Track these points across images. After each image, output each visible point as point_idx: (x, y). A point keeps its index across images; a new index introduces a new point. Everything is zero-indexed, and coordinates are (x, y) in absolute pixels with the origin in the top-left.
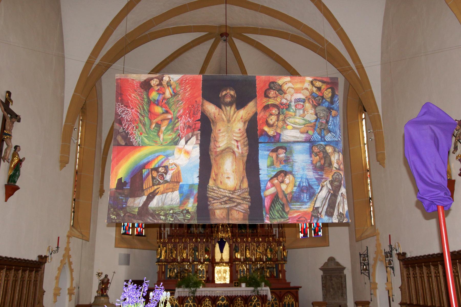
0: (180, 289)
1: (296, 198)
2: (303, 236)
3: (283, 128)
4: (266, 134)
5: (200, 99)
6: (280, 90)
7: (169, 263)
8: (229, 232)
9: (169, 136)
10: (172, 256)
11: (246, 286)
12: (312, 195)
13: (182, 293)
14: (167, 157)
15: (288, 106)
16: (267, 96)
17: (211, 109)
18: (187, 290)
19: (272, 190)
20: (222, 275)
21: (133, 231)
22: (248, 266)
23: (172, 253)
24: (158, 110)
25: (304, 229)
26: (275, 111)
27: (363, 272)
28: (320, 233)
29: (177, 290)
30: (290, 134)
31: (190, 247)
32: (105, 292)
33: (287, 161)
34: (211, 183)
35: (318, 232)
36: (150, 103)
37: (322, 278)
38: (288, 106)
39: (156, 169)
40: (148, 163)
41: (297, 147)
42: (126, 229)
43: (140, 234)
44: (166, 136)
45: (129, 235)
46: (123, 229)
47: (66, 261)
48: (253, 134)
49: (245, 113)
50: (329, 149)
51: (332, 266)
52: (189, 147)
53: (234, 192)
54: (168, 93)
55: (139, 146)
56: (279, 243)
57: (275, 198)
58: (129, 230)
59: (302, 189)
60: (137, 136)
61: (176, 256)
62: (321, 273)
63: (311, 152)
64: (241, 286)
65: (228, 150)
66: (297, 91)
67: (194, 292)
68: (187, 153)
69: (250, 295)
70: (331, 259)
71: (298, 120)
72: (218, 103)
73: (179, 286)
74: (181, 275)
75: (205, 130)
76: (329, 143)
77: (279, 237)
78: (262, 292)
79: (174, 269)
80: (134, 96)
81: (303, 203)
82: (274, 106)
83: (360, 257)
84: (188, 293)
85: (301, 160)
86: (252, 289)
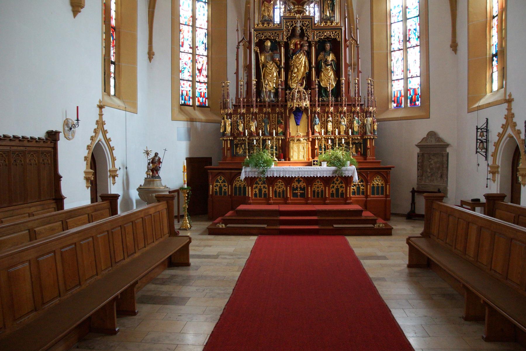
0: (248, 169)
2: (397, 106)
8: (307, 99)
10: (238, 129)
11: (327, 166)
13: (250, 173)
18: (255, 170)
20: (299, 152)
21: (194, 102)
22: (330, 141)
23: (238, 125)
25: (397, 97)
27: (479, 150)
31: (259, 118)
32: (157, 173)
35: (415, 101)
37: (418, 156)
42: (185, 100)
43: (202, 106)
45: (189, 106)
46: (182, 100)
47: (100, 136)
51: (434, 143)
56: (367, 114)
58: (189, 100)
61: (244, 129)
62: (418, 150)
64: (321, 165)
67: (263, 172)
69: (333, 176)
73: (247, 165)
74: (249, 152)
77: (368, 106)
78: (346, 172)
79: (241, 144)
83: (477, 132)
84: (256, 173)
86: (334, 168)
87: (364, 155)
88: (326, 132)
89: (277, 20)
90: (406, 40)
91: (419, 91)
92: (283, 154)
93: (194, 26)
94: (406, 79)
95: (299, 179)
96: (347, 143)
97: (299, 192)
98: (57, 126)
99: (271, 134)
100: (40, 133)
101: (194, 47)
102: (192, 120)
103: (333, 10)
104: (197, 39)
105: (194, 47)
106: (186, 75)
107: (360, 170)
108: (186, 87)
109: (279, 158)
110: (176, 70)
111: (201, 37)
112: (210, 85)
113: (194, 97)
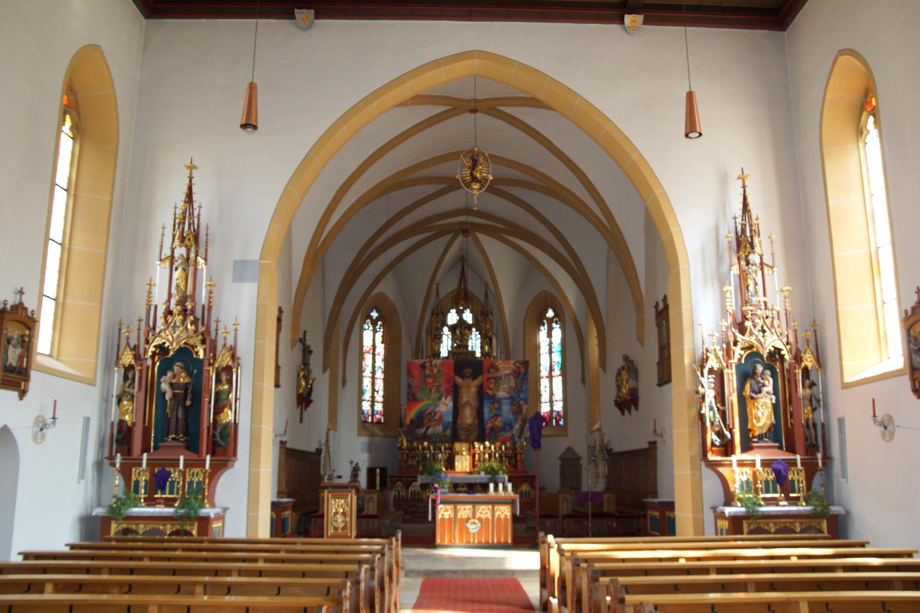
0: (423, 477)
1: (503, 429)
3: (498, 390)
4: (487, 394)
5: (452, 374)
6: (497, 369)
7: (410, 451)
9: (437, 396)
12: (511, 427)
14: (436, 406)
15: (501, 378)
16: (489, 372)
17: (459, 380)
19: (490, 425)
24: (430, 380)
26: (493, 381)
28: (561, 423)
29: (419, 477)
30: (501, 394)
33: (499, 409)
34: (459, 421)
36: (426, 376)
38: (501, 378)
39: (430, 414)
40: (426, 410)
41: (505, 401)
43: (379, 422)
44: (435, 395)
48: (481, 394)
50: (522, 402)
52: (447, 402)
53: (470, 425)
54: (435, 371)
55: (422, 400)
57: (492, 429)
59: (506, 424)
60: (420, 395)
62: (559, 462)
63: (512, 404)
65: (468, 403)
66: (506, 369)
68: (446, 405)
70: (569, 449)
71: (506, 386)
72: (463, 377)
73: (422, 474)
75: (456, 393)
76: (522, 399)
80: (416, 373)
81: (506, 431)
82: (493, 378)
85: (506, 408)
87: (515, 466)
88: (485, 448)
89: (444, 353)
90: (551, 369)
91: (562, 413)
92: (450, 465)
93: (374, 355)
94: (551, 402)
96: (501, 456)
98: (317, 446)
99: (440, 449)
100: (313, 450)
101: (374, 372)
102: (372, 435)
104: (376, 365)
105: (374, 372)
106: (367, 396)
108: (366, 406)
109: (446, 469)
110: (361, 392)
111: (380, 363)
112: (385, 403)
113: (373, 415)
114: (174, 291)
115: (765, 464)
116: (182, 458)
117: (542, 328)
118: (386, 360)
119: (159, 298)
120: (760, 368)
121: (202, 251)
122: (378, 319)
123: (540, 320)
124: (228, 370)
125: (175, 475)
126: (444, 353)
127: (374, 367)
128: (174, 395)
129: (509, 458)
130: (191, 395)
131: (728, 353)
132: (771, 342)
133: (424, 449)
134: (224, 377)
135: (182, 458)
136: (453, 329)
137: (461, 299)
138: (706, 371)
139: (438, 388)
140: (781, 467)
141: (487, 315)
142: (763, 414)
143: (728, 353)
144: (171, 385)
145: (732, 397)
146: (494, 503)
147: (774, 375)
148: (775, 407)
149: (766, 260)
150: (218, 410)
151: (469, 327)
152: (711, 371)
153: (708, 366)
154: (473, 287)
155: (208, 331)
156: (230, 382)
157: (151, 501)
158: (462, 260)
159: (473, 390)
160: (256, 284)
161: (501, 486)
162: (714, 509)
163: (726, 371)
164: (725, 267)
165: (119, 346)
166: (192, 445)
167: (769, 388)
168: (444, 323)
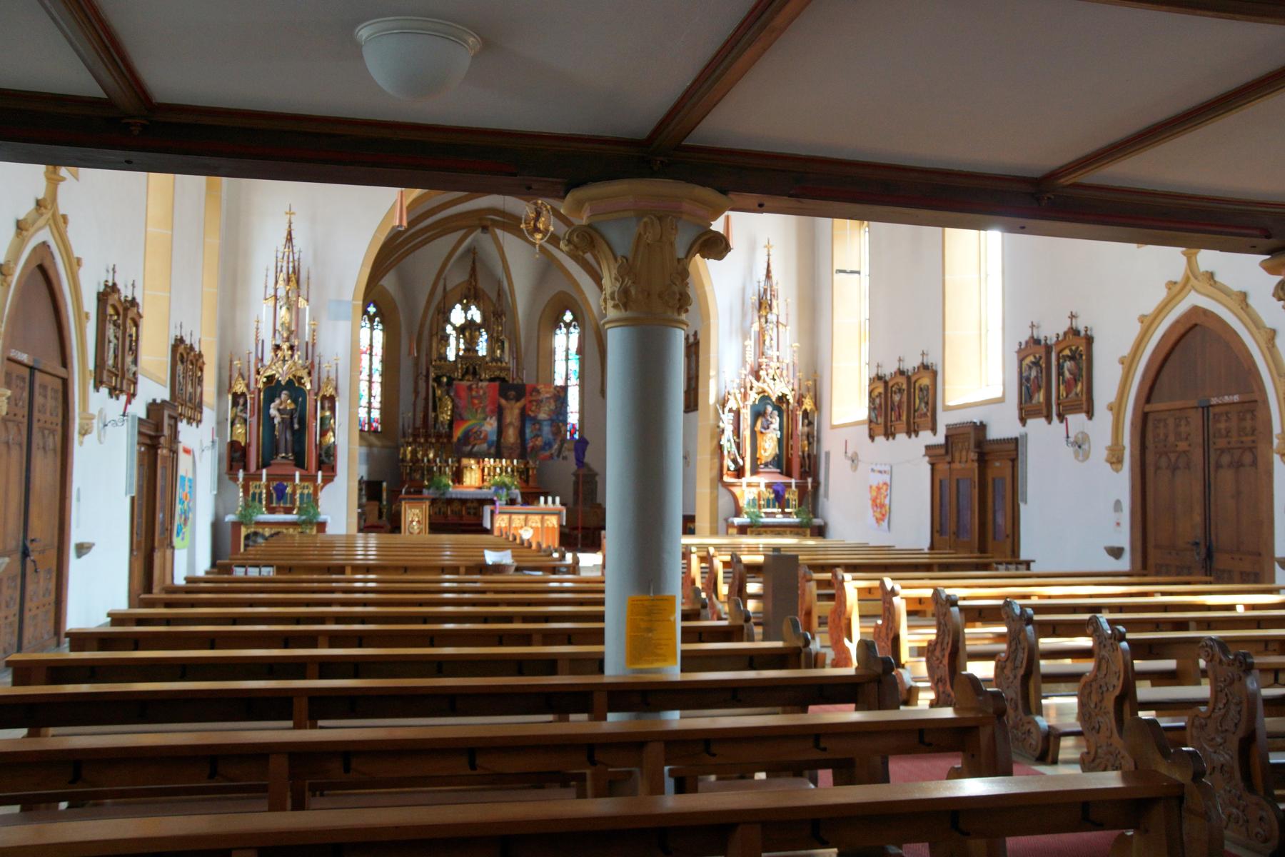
1: (543, 448)
6: (538, 392)
17: (503, 402)
30: (542, 416)
33: (540, 429)
36: (473, 398)
43: (376, 431)
44: (480, 416)
48: (524, 416)
49: (519, 404)
57: (533, 448)
60: (466, 415)
62: (573, 478)
63: (551, 426)
65: (511, 424)
72: (507, 399)
73: (428, 487)
75: (500, 413)
85: (546, 429)
87: (527, 481)
89: (451, 355)
92: (458, 477)
93: (371, 355)
95: (472, 501)
97: (472, 511)
99: (447, 461)
101: (370, 376)
102: (370, 446)
103: (503, 351)
105: (370, 376)
107: (522, 494)
109: (454, 482)
111: (377, 366)
112: (383, 410)
114: (278, 327)
115: (768, 486)
116: (297, 474)
117: (558, 331)
118: (384, 361)
119: (266, 334)
120: (769, 409)
121: (303, 291)
122: (376, 315)
123: (556, 322)
124: (332, 399)
125: (289, 490)
126: (451, 355)
127: (371, 369)
128: (283, 419)
129: (521, 473)
130: (297, 423)
131: (745, 396)
132: (777, 389)
133: (429, 461)
134: (327, 405)
135: (297, 474)
136: (461, 330)
137: (471, 295)
138: (726, 410)
139: (484, 408)
140: (779, 488)
141: (500, 316)
142: (769, 447)
143: (745, 396)
144: (279, 410)
145: (746, 433)
146: (543, 514)
147: (780, 416)
148: (780, 441)
149: (782, 320)
150: (323, 434)
151: (479, 327)
152: (730, 410)
153: (728, 406)
154: (482, 284)
155: (312, 364)
156: (333, 409)
157: (272, 510)
158: (472, 252)
159: (516, 411)
160: (349, 323)
161: (550, 499)
162: (726, 520)
163: (742, 411)
164: (748, 323)
165: (231, 377)
166: (300, 462)
167: (776, 425)
168: (448, 321)
